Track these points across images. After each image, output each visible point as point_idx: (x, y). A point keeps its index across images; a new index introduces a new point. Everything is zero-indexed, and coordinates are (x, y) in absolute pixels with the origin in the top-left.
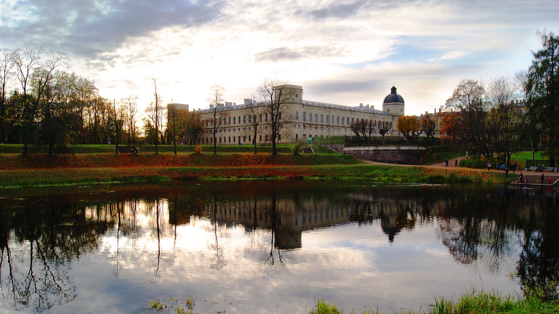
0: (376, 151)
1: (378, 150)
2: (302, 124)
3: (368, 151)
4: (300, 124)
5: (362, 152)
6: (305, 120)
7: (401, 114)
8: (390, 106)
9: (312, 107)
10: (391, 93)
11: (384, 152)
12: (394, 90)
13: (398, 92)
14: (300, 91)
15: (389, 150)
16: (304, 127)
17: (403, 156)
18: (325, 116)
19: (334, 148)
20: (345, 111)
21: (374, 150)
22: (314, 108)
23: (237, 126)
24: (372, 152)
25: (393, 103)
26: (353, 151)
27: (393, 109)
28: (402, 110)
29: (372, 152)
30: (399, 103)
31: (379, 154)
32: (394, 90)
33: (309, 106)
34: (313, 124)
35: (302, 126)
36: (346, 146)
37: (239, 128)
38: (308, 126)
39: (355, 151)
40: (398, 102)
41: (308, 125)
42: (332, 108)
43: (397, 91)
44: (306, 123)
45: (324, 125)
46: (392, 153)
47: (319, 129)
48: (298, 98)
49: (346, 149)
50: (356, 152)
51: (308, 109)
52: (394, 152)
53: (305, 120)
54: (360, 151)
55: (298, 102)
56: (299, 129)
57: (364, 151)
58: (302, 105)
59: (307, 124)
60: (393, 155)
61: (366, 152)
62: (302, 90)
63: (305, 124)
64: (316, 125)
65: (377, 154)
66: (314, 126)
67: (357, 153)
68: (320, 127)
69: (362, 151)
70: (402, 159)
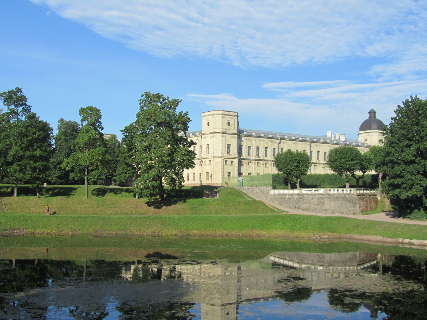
1: (303, 195)
3: (292, 195)
5: (287, 196)
11: (310, 196)
15: (316, 195)
19: (261, 191)
21: (298, 194)
24: (296, 196)
26: (278, 195)
29: (296, 196)
31: (304, 200)
36: (275, 188)
39: (280, 195)
49: (272, 192)
50: (281, 196)
54: (285, 195)
57: (290, 195)
60: (320, 201)
61: (291, 196)
65: (301, 200)
67: (282, 198)
70: (331, 207)
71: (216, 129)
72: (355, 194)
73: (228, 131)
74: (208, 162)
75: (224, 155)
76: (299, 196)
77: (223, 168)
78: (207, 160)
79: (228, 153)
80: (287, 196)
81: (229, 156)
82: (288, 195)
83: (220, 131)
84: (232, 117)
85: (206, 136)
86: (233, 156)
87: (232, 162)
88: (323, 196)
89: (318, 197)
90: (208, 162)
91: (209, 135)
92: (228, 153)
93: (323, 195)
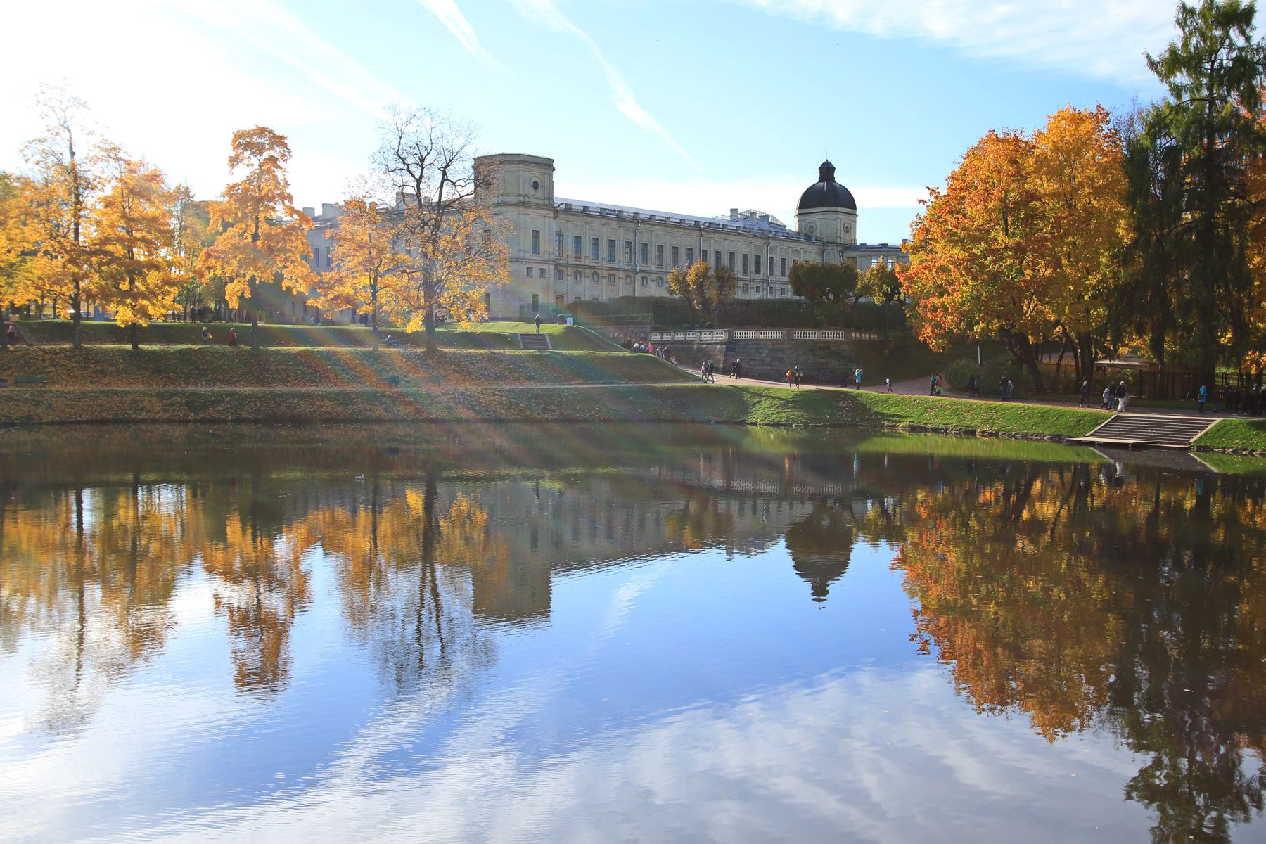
2: (552, 267)
4: (545, 267)
7: (846, 239)
8: (815, 217)
10: (821, 180)
12: (827, 171)
13: (840, 178)
16: (559, 274)
18: (621, 242)
20: (682, 231)
22: (589, 220)
24: (718, 346)
25: (824, 209)
27: (825, 221)
28: (850, 229)
30: (839, 209)
32: (827, 171)
33: (575, 213)
34: (585, 267)
36: (655, 330)
40: (837, 205)
41: (569, 269)
42: (643, 222)
43: (836, 175)
45: (618, 270)
47: (605, 281)
48: (540, 192)
51: (570, 225)
58: (551, 213)
62: (554, 169)
63: (560, 264)
64: (594, 268)
66: (587, 271)
68: (605, 273)
71: (507, 195)
79: (536, 248)
81: (535, 258)
87: (542, 270)
92: (536, 248)
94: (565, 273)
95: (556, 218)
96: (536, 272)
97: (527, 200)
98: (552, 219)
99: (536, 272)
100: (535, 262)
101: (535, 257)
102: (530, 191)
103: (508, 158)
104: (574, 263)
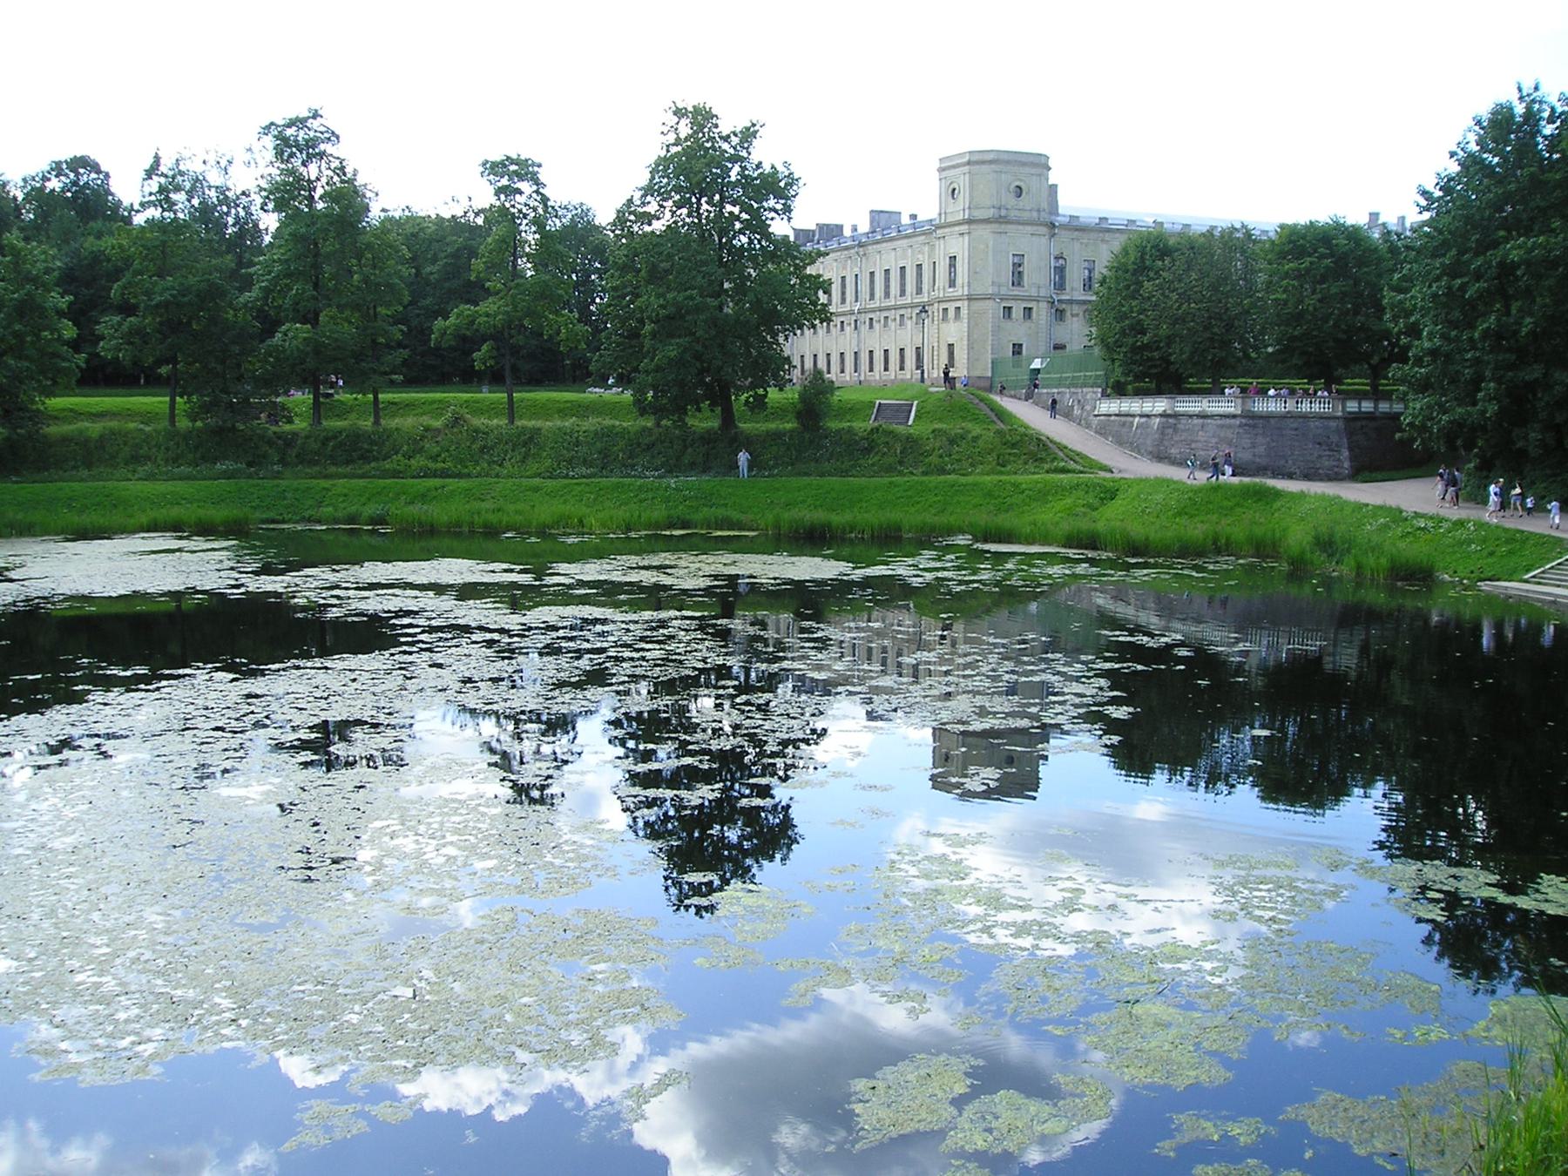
0: (1169, 416)
1: (1176, 416)
2: (1044, 305)
6: (1060, 286)
9: (1093, 235)
11: (1196, 421)
14: (1039, 171)
16: (1060, 314)
17: (1260, 439)
21: (1164, 415)
22: (1107, 236)
23: (896, 308)
35: (1042, 312)
36: (1119, 390)
37: (902, 312)
38: (1076, 309)
44: (1064, 297)
46: (1222, 426)
48: (1025, 201)
52: (1228, 421)
53: (1060, 286)
55: (1026, 216)
56: (1028, 323)
58: (1044, 230)
59: (1071, 302)
67: (1124, 424)
69: (1133, 416)
71: (977, 208)
72: (1340, 414)
73: (1013, 214)
74: (951, 313)
75: (1004, 291)
76: (1164, 420)
77: (997, 330)
78: (951, 307)
80: (1137, 419)
82: (1141, 416)
83: (990, 213)
84: (1027, 170)
85: (947, 230)
86: (1034, 292)
88: (1233, 421)
89: (1219, 422)
90: (951, 313)
91: (957, 228)
93: (1234, 416)
94: (1068, 314)
95: (1054, 235)
96: (1017, 312)
97: (1003, 213)
98: (1044, 240)
99: (1017, 312)
100: (1015, 298)
101: (1016, 291)
102: (1011, 201)
103: (975, 158)
104: (1083, 298)
